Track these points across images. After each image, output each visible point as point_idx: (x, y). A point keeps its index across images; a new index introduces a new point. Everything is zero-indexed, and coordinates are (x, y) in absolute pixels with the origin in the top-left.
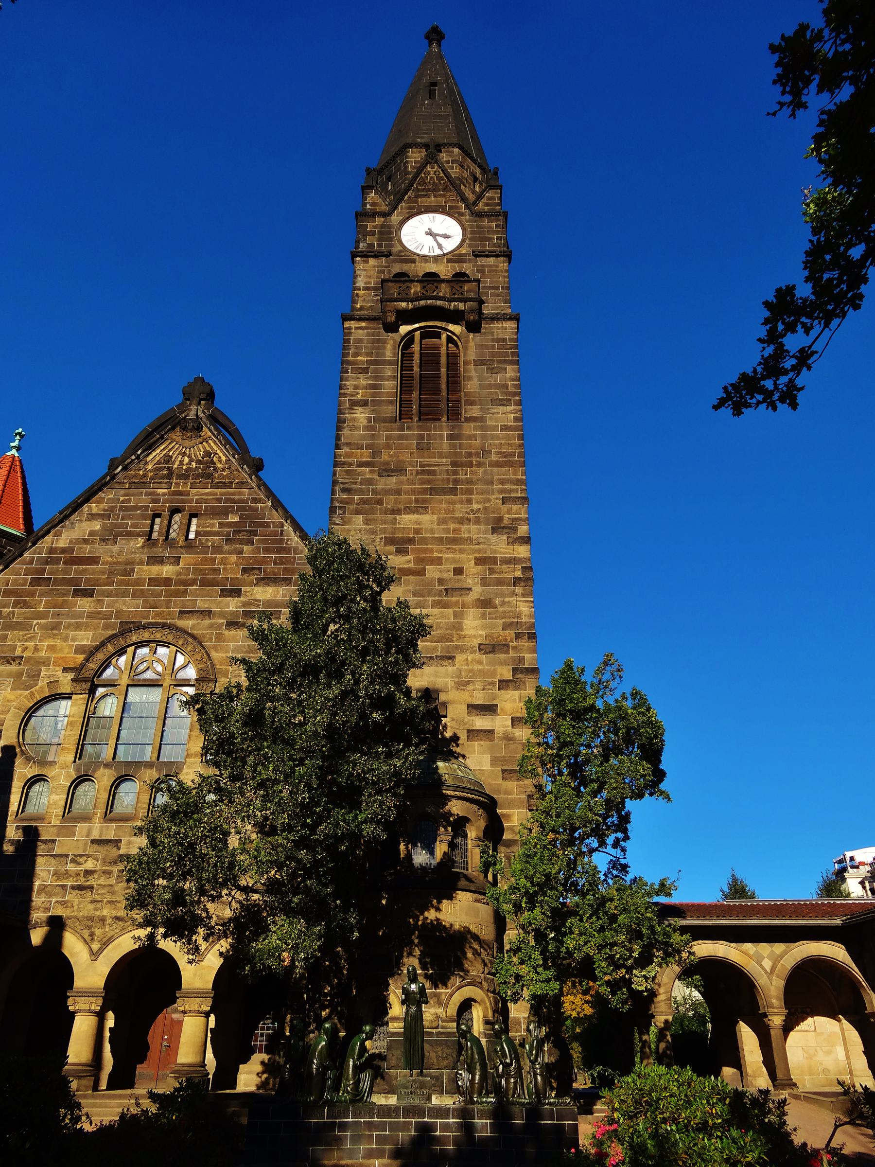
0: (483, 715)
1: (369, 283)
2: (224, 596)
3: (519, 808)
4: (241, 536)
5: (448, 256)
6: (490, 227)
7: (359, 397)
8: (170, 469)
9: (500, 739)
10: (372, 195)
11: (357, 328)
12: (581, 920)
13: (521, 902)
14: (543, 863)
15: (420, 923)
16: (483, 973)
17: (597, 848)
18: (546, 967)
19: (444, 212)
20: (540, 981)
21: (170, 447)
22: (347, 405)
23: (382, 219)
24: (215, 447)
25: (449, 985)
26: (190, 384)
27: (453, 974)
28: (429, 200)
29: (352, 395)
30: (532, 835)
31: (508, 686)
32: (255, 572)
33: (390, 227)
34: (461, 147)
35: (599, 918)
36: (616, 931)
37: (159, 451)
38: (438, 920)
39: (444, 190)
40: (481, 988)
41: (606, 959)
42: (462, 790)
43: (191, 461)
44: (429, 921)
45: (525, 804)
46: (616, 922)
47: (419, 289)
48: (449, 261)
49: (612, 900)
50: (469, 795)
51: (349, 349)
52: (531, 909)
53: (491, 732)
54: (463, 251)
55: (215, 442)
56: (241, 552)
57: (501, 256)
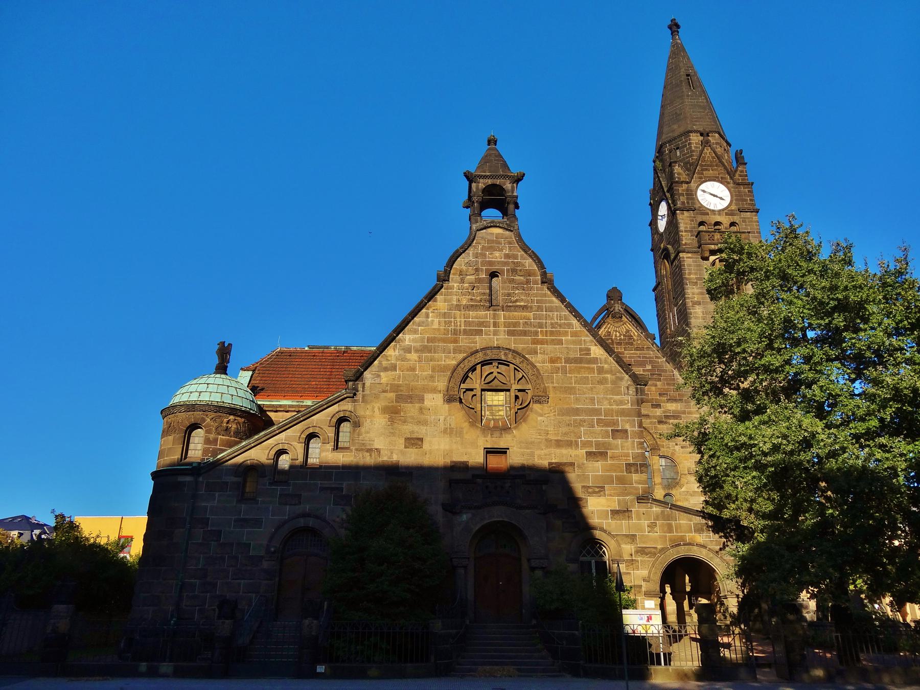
1: (687, 227)
2: (654, 408)
4: (655, 377)
5: (726, 211)
6: (745, 192)
7: (696, 299)
8: (612, 339)
10: (677, 167)
11: (687, 258)
19: (718, 181)
21: (608, 326)
22: (691, 304)
23: (686, 185)
24: (630, 327)
26: (609, 291)
28: (709, 172)
29: (692, 298)
32: (665, 395)
33: (691, 191)
34: (719, 134)
37: (603, 329)
39: (716, 166)
43: (621, 335)
47: (719, 237)
48: (727, 214)
51: (685, 270)
54: (733, 207)
55: (630, 324)
56: (656, 385)
57: (754, 212)
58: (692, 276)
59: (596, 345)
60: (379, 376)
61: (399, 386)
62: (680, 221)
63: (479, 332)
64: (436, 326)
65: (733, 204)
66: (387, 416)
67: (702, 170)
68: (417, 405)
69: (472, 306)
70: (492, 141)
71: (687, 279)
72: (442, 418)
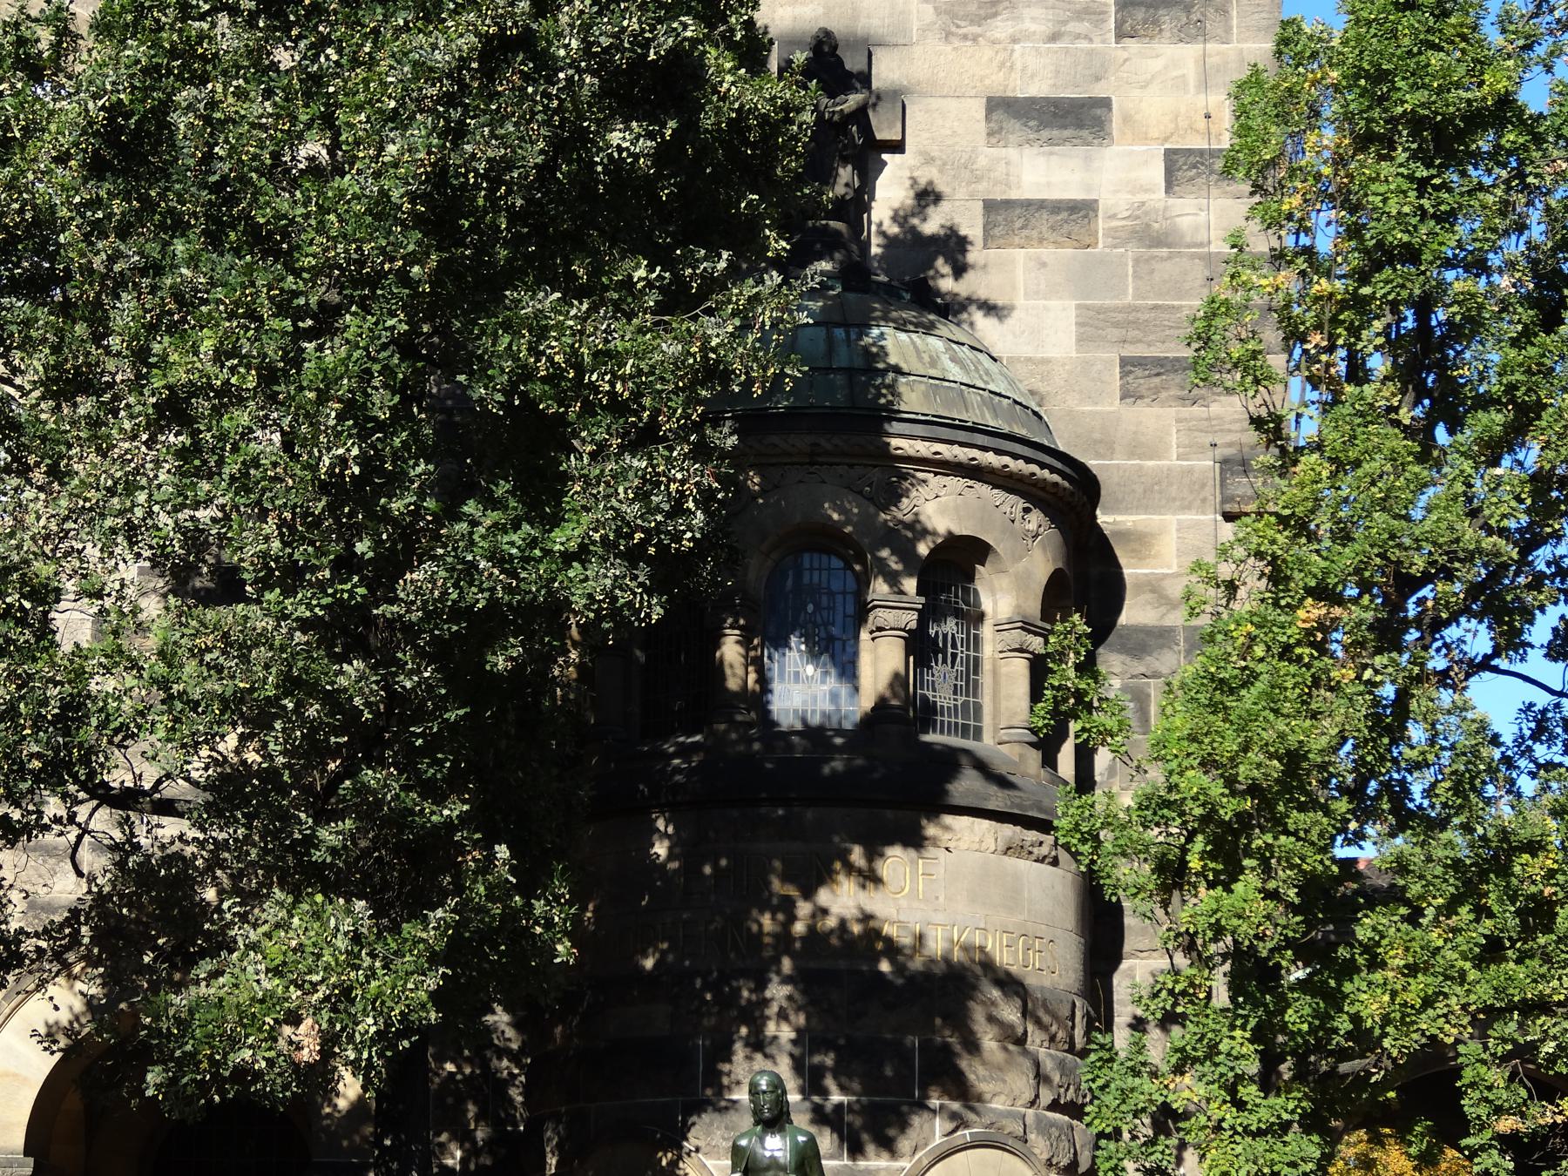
0: (1050, 142)
3: (1186, 508)
9: (1119, 238)
12: (1414, 918)
13: (1184, 850)
14: (1276, 712)
15: (799, 928)
16: (1032, 1103)
17: (1487, 658)
18: (1268, 1082)
20: (1247, 1131)
25: (904, 1144)
27: (921, 1106)
30: (1235, 606)
31: (1156, 22)
35: (1482, 912)
36: (1547, 959)
38: (866, 918)
40: (1026, 1157)
41: (1505, 1059)
42: (962, 436)
44: (831, 922)
45: (1208, 492)
46: (1548, 929)
49: (1534, 847)
50: (990, 459)
52: (1226, 879)
53: (1082, 210)
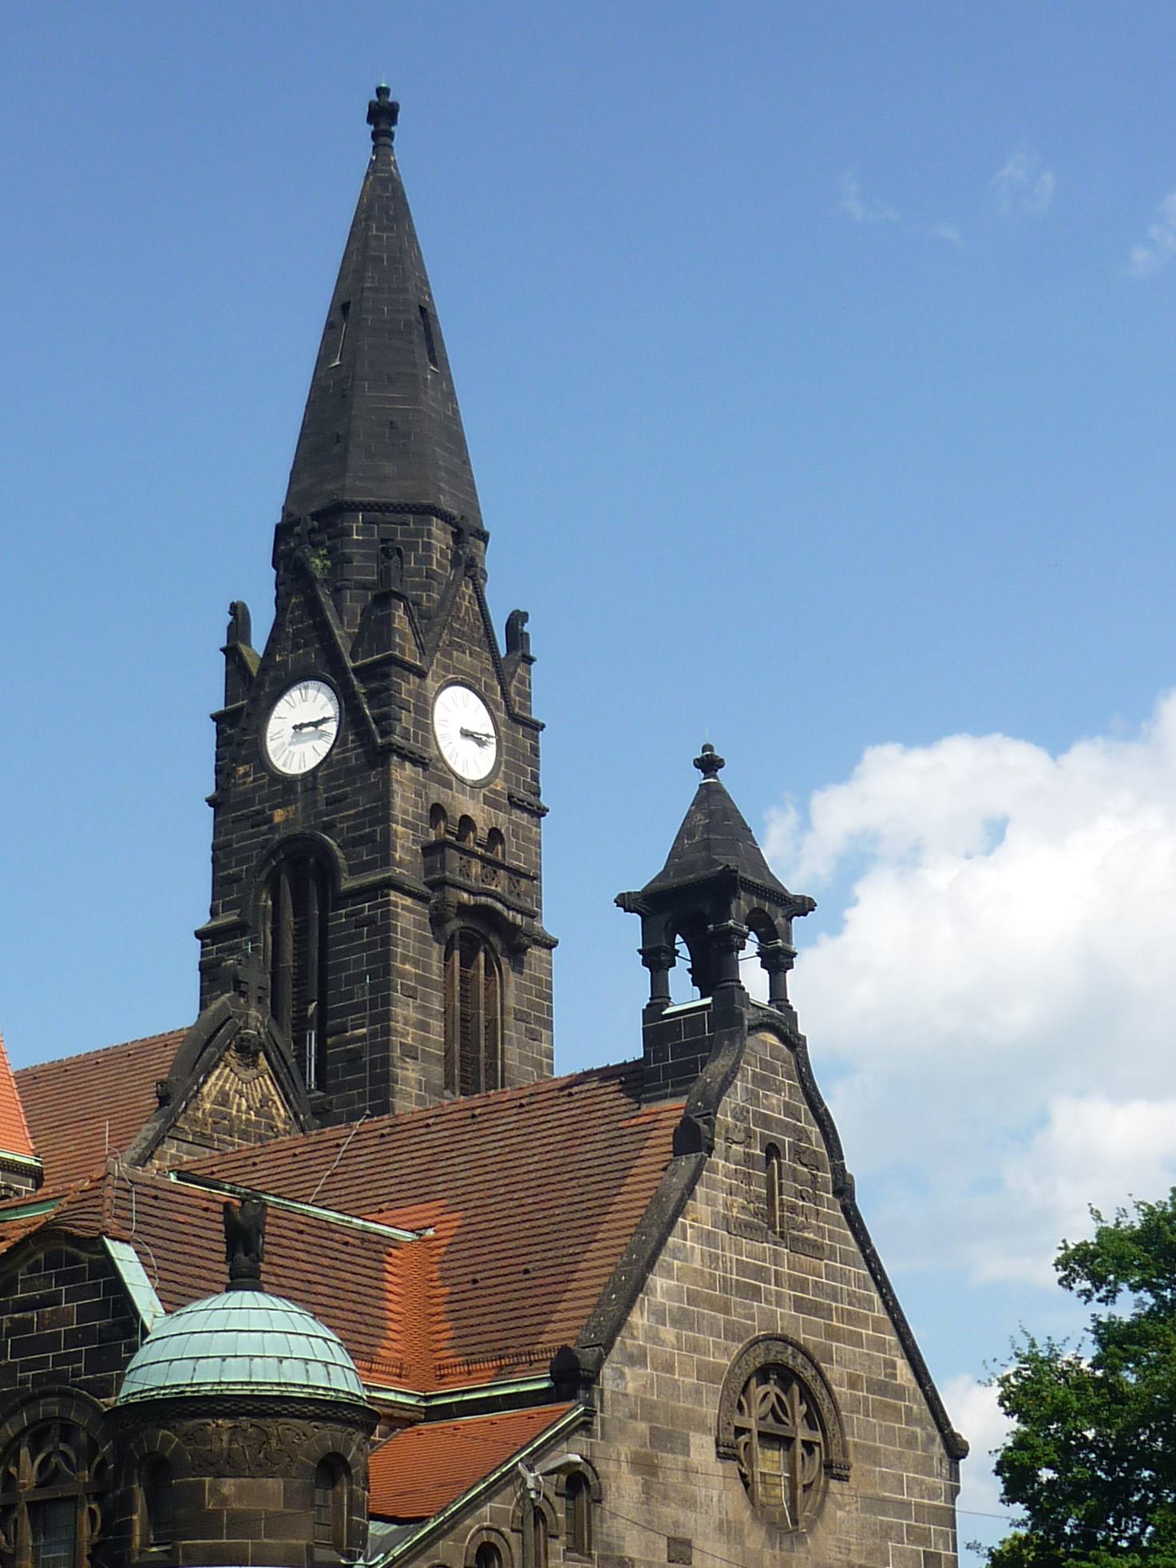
24: (271, 1088)
43: (249, 1108)
58: (407, 967)
59: (903, 1358)
60: (622, 1375)
61: (653, 1406)
62: (395, 786)
63: (755, 1293)
64: (697, 1265)
65: (501, 775)
66: (639, 1478)
67: (451, 643)
68: (681, 1458)
69: (748, 1225)
70: (709, 764)
71: (402, 974)
72: (715, 1494)
